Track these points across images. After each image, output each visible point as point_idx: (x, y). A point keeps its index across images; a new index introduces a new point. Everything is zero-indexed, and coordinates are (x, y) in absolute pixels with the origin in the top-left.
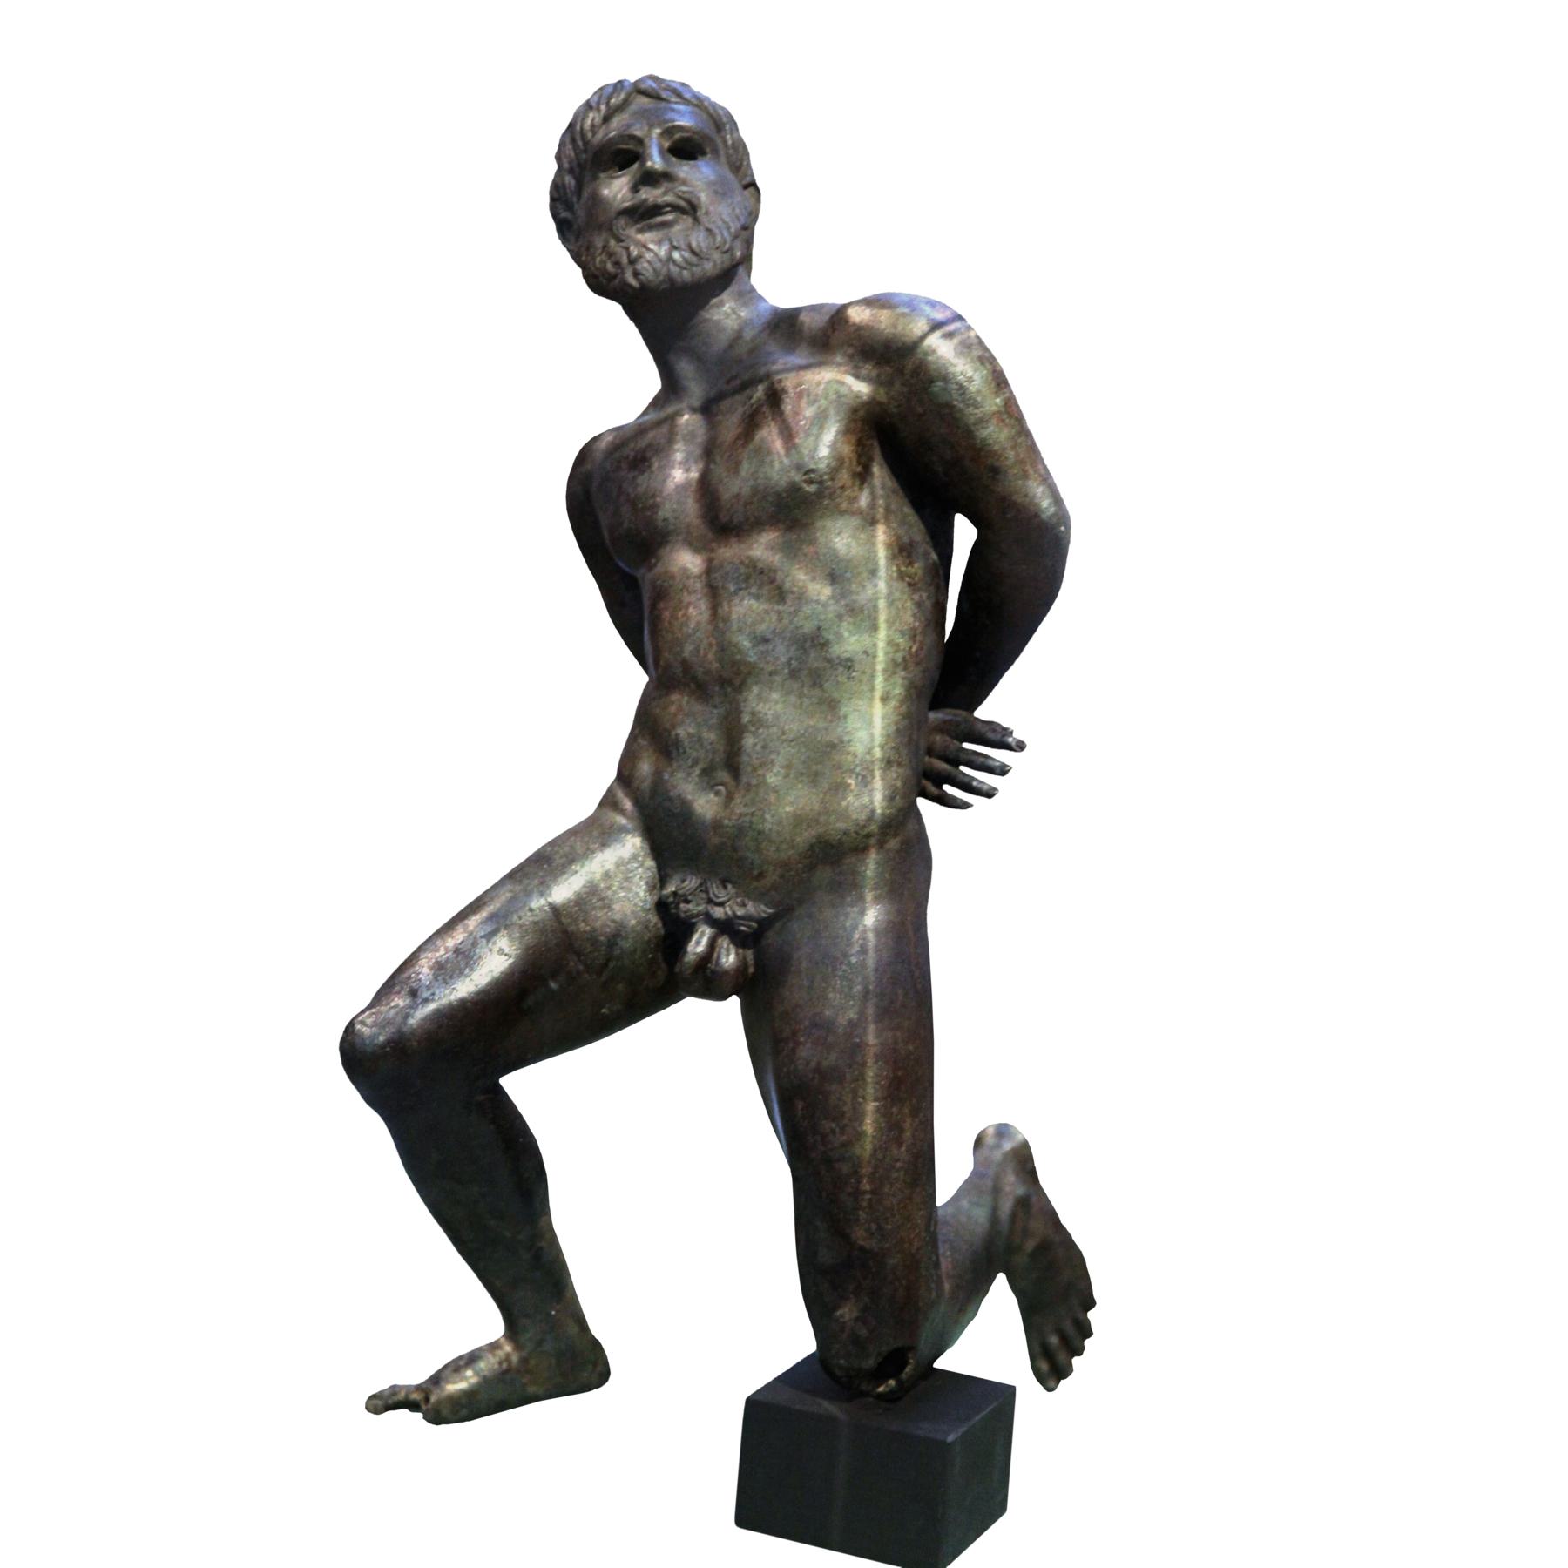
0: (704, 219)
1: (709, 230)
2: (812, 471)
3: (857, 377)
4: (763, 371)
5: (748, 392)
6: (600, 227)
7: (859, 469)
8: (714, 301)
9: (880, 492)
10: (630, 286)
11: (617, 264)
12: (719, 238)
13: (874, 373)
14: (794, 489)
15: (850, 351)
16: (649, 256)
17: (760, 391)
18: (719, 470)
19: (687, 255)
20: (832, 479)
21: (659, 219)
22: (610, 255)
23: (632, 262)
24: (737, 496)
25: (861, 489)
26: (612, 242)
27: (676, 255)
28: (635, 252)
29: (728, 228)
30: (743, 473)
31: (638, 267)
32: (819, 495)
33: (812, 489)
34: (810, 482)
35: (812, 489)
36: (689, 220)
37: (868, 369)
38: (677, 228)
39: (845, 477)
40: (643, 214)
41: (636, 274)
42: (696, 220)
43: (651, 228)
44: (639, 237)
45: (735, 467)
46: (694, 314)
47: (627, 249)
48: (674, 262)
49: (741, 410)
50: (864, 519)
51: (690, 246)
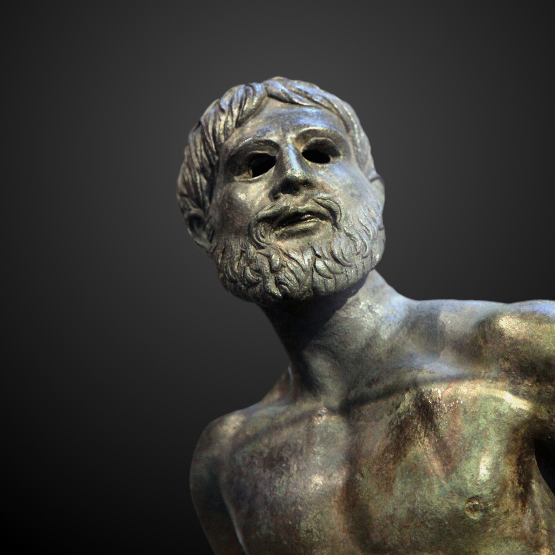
0: (344, 225)
1: (349, 235)
2: (476, 498)
3: (515, 393)
4: (408, 377)
5: (392, 400)
6: (238, 232)
7: (520, 489)
8: (350, 300)
9: (541, 512)
10: (273, 295)
11: (258, 271)
12: (359, 243)
13: (535, 390)
14: (457, 517)
15: (507, 365)
16: (292, 265)
17: (407, 400)
18: (368, 485)
19: (330, 263)
20: (497, 506)
21: (301, 226)
22: (250, 261)
23: (273, 271)
24: (392, 517)
25: (524, 512)
26: (252, 249)
27: (320, 264)
28: (277, 260)
29: (367, 231)
30: (397, 493)
31: (281, 276)
32: (484, 522)
33: (476, 516)
34: (474, 509)
35: (476, 516)
36: (328, 225)
37: (526, 385)
38: (317, 236)
39: (508, 501)
40: (285, 222)
41: (278, 283)
42: (335, 224)
43: (292, 235)
44: (279, 243)
45: (387, 484)
46: (333, 312)
47: (269, 257)
48: (318, 271)
49: (387, 418)
50: (528, 544)
51: (332, 253)
